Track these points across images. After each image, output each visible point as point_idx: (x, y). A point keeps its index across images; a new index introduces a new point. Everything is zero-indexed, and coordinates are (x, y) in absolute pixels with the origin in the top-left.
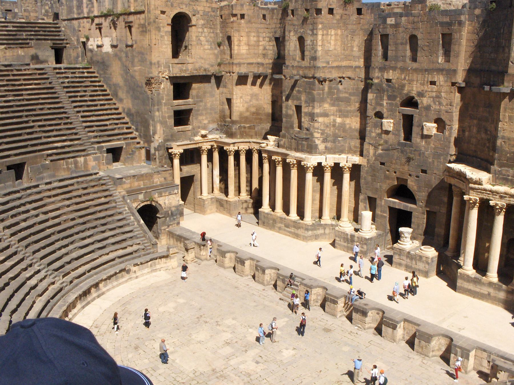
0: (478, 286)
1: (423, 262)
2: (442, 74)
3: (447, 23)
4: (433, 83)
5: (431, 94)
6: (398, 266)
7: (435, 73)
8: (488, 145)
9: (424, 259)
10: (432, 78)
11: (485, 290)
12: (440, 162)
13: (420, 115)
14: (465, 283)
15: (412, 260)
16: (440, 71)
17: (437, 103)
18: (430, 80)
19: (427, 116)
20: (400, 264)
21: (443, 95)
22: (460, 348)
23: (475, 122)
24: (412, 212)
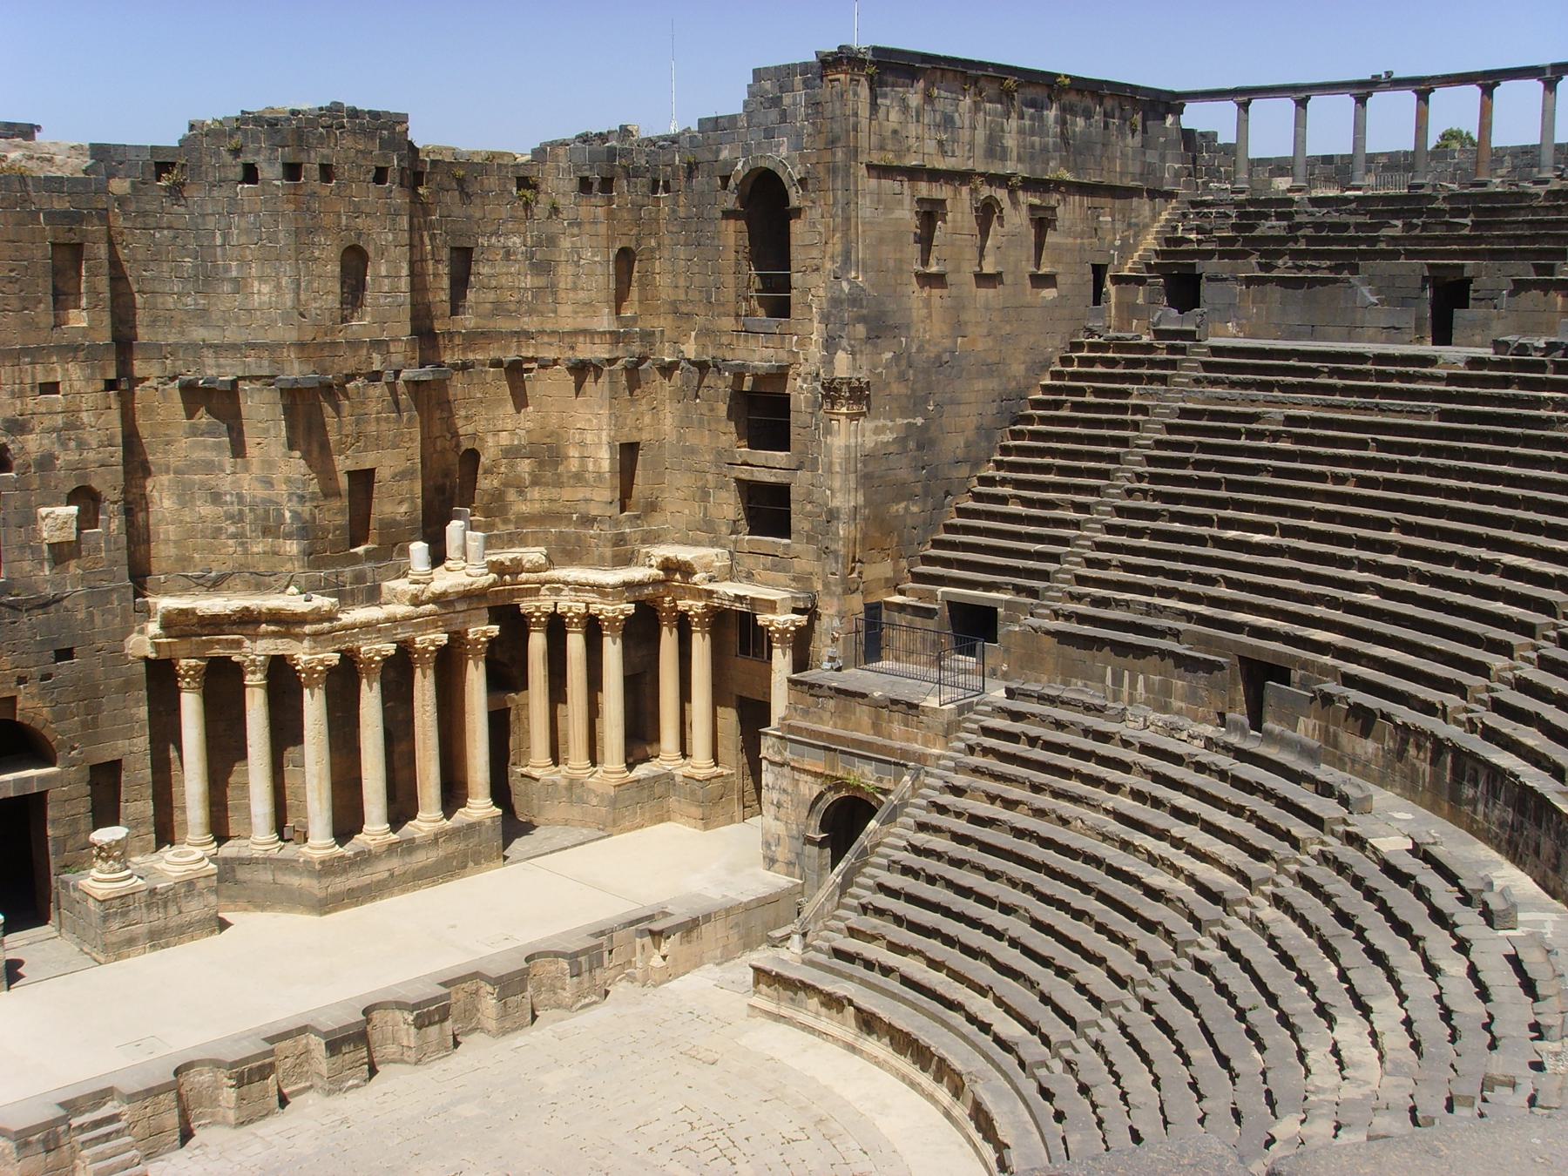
0: (368, 870)
1: (201, 894)
2: (74, 359)
3: (65, 214)
4: (52, 388)
5: (48, 422)
6: (125, 950)
7: (54, 359)
8: (232, 529)
9: (201, 884)
10: (49, 371)
11: (380, 871)
12: (109, 611)
13: (23, 486)
14: (338, 880)
15: (165, 907)
16: (70, 350)
17: (72, 444)
18: (41, 379)
19: (44, 485)
20: (131, 942)
21: (85, 420)
22: (585, 951)
23: (165, 479)
24: (42, 796)
